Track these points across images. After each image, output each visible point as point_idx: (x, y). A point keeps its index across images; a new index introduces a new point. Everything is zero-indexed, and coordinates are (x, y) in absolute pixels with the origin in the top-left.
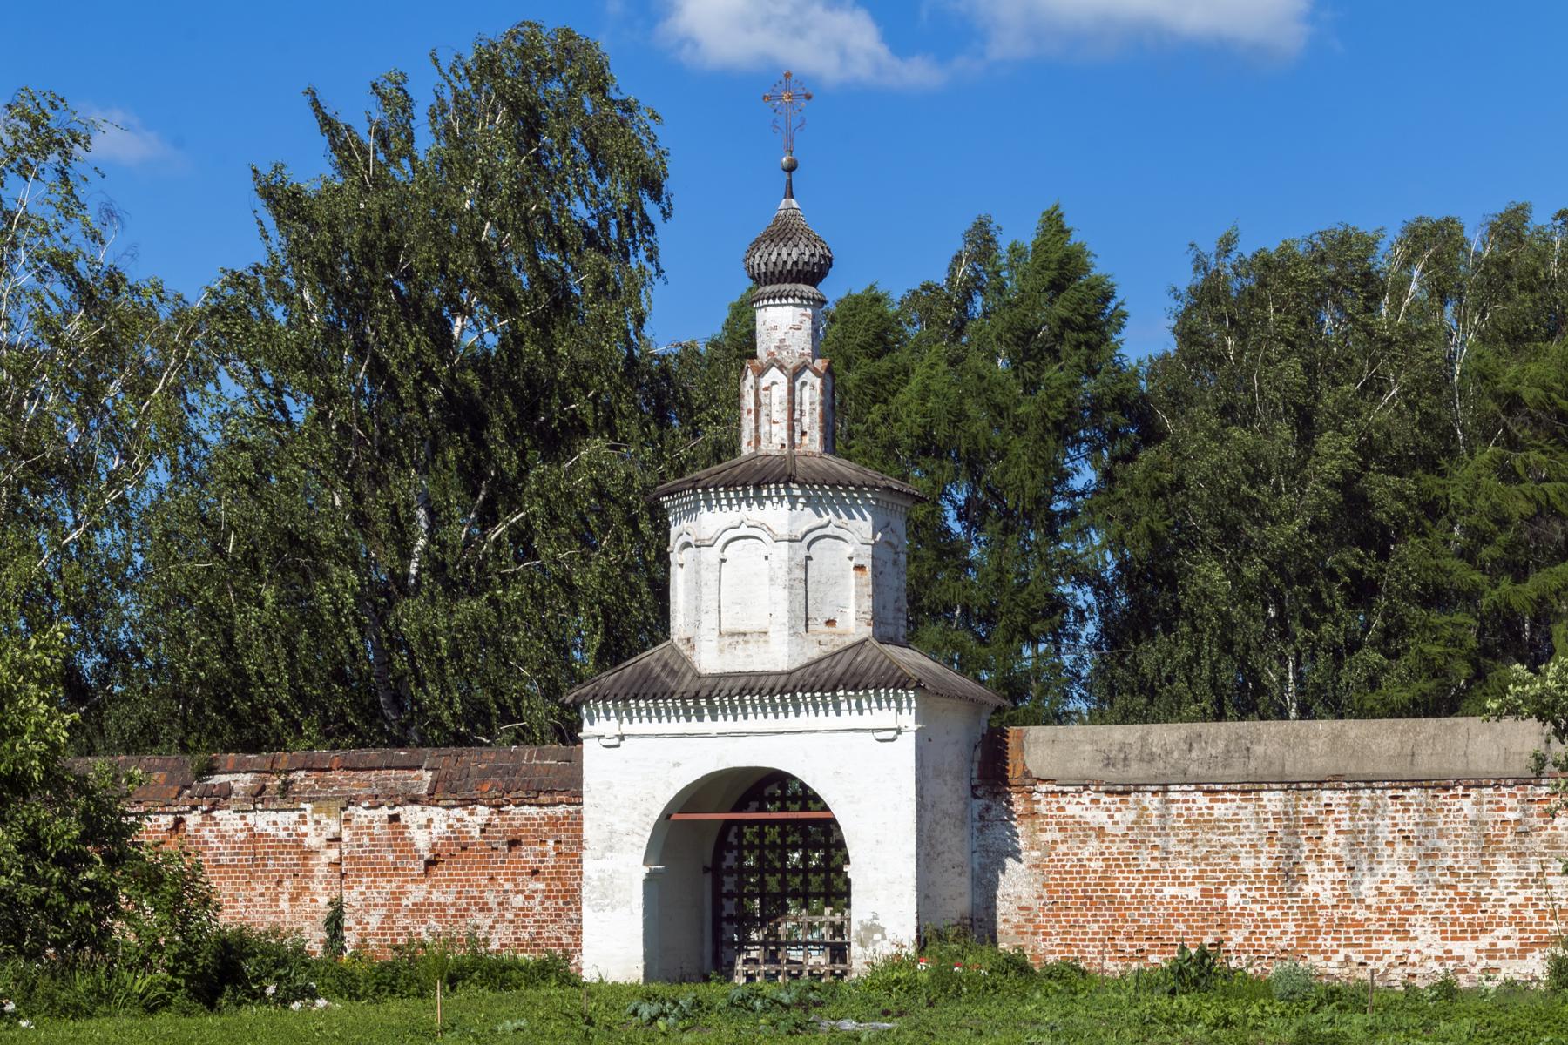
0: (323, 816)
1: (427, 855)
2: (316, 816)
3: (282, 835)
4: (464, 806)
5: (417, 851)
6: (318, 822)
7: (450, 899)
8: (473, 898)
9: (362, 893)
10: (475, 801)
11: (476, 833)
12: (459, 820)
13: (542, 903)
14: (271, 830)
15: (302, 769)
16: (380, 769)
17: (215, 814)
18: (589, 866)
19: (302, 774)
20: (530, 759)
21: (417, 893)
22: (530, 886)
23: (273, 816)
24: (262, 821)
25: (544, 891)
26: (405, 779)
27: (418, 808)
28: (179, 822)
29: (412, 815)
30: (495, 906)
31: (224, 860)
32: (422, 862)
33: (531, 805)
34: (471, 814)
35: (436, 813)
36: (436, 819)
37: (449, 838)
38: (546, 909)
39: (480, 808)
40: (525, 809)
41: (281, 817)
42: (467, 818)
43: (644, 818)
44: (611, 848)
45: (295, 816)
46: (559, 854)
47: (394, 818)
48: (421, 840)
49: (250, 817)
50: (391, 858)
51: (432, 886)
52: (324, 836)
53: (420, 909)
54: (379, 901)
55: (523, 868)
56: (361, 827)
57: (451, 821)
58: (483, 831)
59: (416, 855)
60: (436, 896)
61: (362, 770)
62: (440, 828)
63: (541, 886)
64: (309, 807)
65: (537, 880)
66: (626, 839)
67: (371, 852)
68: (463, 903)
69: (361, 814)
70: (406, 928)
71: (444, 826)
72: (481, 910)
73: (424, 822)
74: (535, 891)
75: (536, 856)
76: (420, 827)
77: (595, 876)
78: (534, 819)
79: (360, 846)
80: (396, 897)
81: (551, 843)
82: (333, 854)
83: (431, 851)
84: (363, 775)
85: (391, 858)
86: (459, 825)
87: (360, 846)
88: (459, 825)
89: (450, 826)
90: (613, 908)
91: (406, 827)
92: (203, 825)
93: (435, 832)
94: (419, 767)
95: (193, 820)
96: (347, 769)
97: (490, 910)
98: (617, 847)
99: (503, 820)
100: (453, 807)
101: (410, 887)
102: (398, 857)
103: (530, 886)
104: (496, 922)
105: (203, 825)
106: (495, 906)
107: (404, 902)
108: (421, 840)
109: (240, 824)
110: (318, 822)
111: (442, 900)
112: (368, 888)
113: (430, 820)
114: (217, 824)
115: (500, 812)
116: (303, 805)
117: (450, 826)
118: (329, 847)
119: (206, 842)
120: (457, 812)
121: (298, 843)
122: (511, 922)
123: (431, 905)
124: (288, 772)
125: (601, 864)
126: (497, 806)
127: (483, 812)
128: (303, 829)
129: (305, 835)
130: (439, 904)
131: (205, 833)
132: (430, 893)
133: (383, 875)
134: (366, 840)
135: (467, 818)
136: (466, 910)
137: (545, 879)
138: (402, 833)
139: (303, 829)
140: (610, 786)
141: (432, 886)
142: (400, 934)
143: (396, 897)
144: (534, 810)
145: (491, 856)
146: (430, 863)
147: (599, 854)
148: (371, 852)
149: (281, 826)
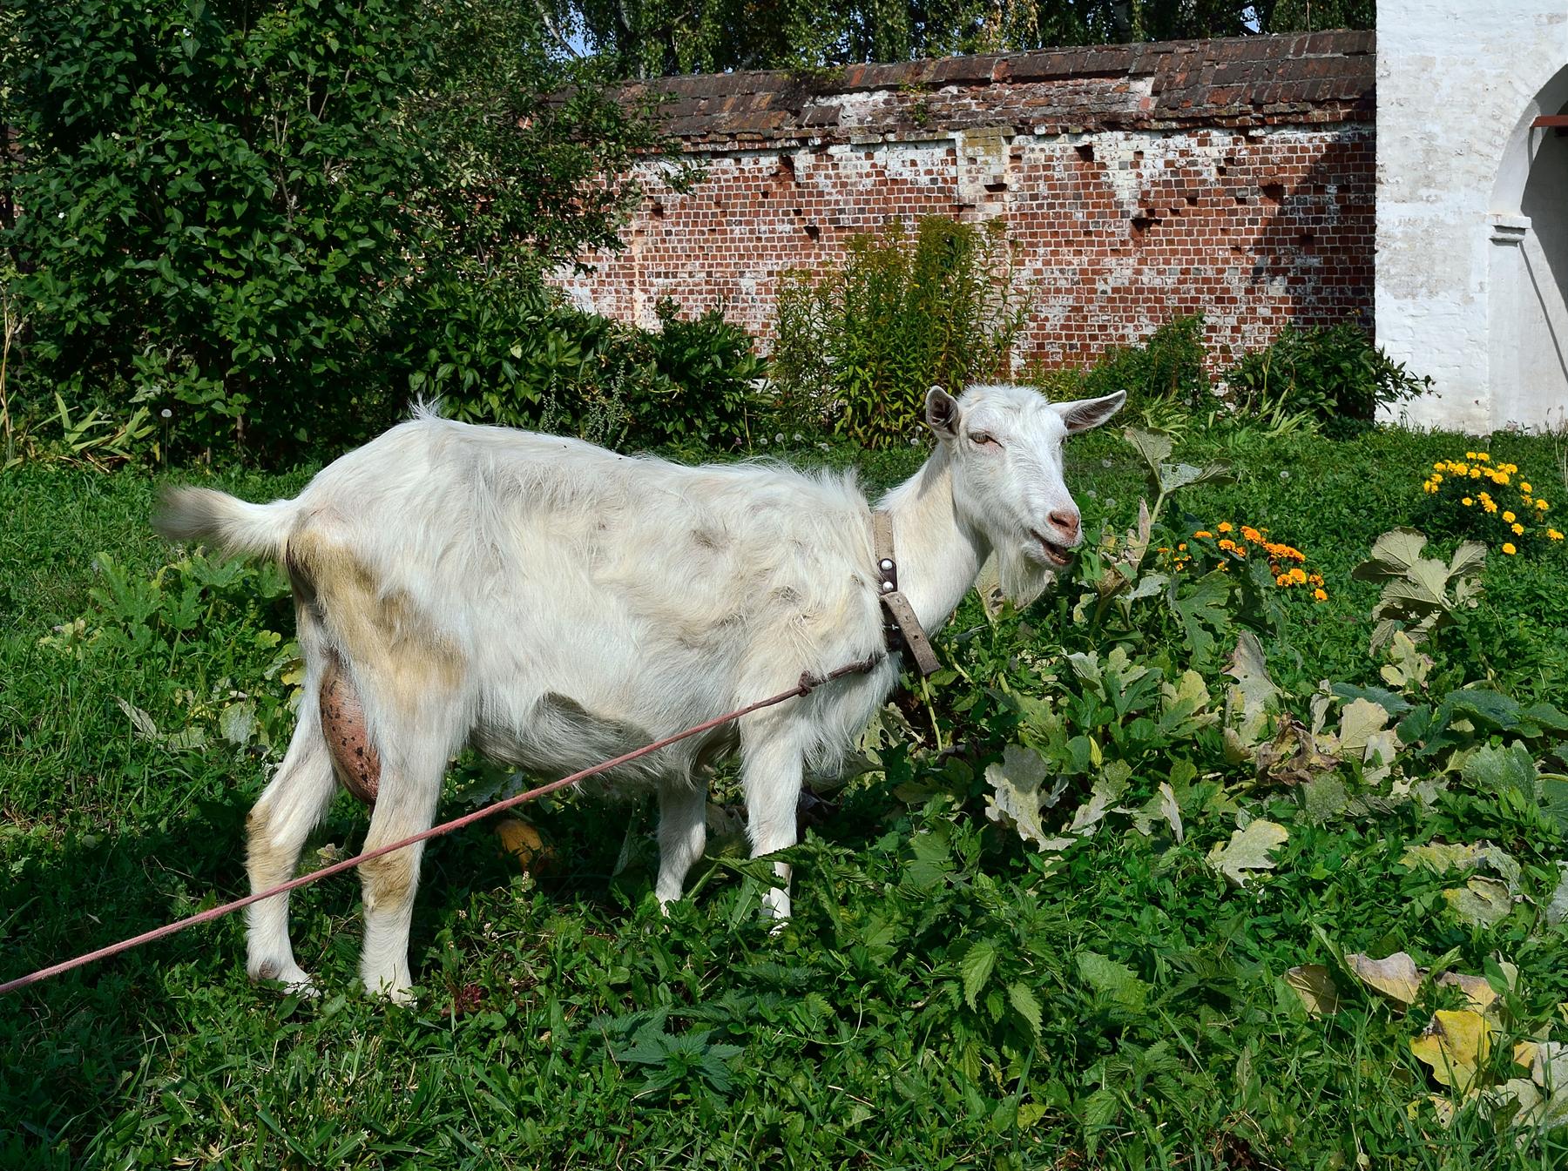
0: (980, 150)
1: (1135, 210)
2: (970, 152)
3: (924, 180)
4: (1188, 131)
5: (1120, 204)
6: (973, 160)
7: (1170, 282)
8: (1206, 281)
9: (1038, 272)
10: (1209, 123)
11: (1211, 174)
12: (1183, 153)
13: (1317, 291)
14: (908, 174)
15: (949, 82)
16: (1065, 77)
17: (832, 150)
18: (1389, 212)
19: (954, 89)
20: (1298, 52)
21: (1120, 272)
22: (1298, 261)
23: (911, 154)
24: (894, 160)
25: (1318, 271)
26: (1103, 91)
27: (1120, 135)
28: (788, 164)
29: (1111, 146)
30: (1240, 295)
31: (846, 219)
32: (1127, 222)
33: (1298, 126)
34: (1202, 143)
35: (1143, 142)
36: (1148, 152)
37: (1167, 183)
38: (1324, 301)
39: (1215, 135)
40: (1288, 134)
41: (920, 155)
42: (1197, 150)
43: (1495, 125)
44: (1428, 181)
45: (940, 152)
46: (1345, 209)
47: (1086, 153)
48: (1125, 186)
49: (880, 156)
50: (1079, 216)
51: (1142, 261)
52: (981, 183)
53: (1126, 299)
54: (1063, 284)
55: (1286, 231)
56: (1035, 168)
57: (1170, 156)
58: (1221, 171)
59: (1118, 210)
60: (1149, 278)
61: (1038, 79)
62: (1153, 166)
63: (1315, 262)
64: (958, 136)
65: (1310, 252)
66: (1454, 162)
67: (1051, 206)
68: (1190, 289)
69: (1036, 150)
70: (1103, 328)
71: (1160, 164)
72: (1219, 300)
73: (1130, 157)
74: (1306, 271)
75: (1306, 211)
76: (1123, 166)
77: (1398, 232)
78: (1304, 150)
79: (1034, 197)
80: (1088, 277)
81: (1332, 189)
82: (994, 209)
83: (1142, 202)
84: (1042, 88)
85: (1079, 216)
86: (1182, 161)
87: (1034, 197)
88: (1182, 161)
89: (1169, 164)
90: (1431, 293)
91: (1103, 166)
92: (816, 167)
93: (1146, 173)
94: (1124, 73)
95: (803, 160)
96: (1017, 79)
97: (1233, 300)
98: (1440, 178)
99: (1254, 152)
100: (1174, 132)
101: (1110, 261)
102: (1091, 215)
103: (1298, 261)
104: (1242, 321)
105: (816, 167)
106: (1240, 295)
107: (1100, 286)
108: (1125, 186)
109: (866, 166)
110: (973, 160)
111: (1157, 282)
112: (1047, 263)
113: (1140, 154)
114: (835, 166)
115: (1252, 140)
116: (951, 135)
117: (1169, 164)
118: (989, 198)
119: (821, 194)
120: (1180, 141)
121: (947, 194)
122: (1267, 321)
123: (1140, 291)
124: (936, 86)
125: (1407, 210)
126: (1244, 130)
127: (1221, 141)
128: (952, 171)
129: (955, 180)
130: (1152, 290)
131: (820, 179)
132: (1138, 272)
133: (1069, 243)
134: (1042, 188)
135: (1197, 150)
136: (1195, 300)
137: (1322, 251)
138: (1096, 176)
139: (952, 171)
140: (1426, 64)
141: (1142, 261)
142: (1094, 338)
143: (1088, 277)
144: (1302, 136)
145: (1233, 212)
146: (1140, 224)
147: (1406, 191)
148: (1051, 206)
149: (922, 169)
